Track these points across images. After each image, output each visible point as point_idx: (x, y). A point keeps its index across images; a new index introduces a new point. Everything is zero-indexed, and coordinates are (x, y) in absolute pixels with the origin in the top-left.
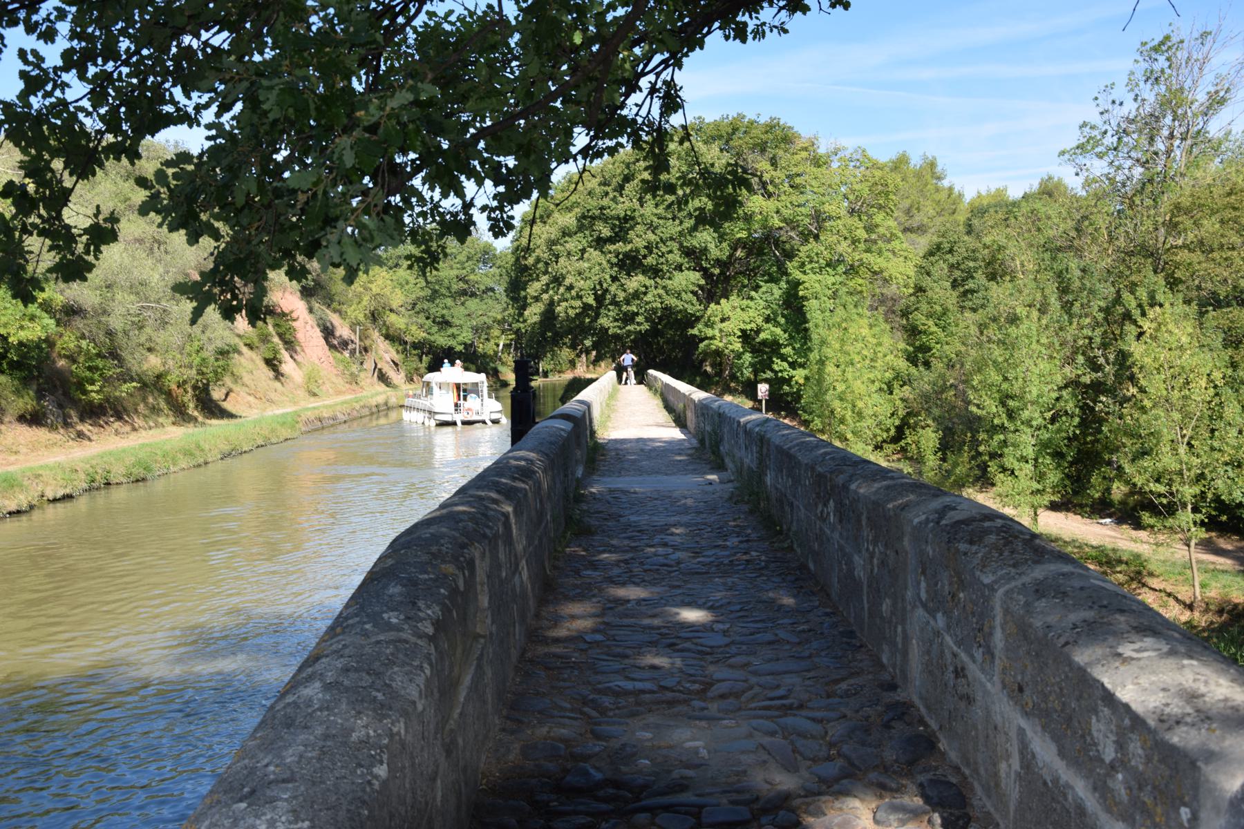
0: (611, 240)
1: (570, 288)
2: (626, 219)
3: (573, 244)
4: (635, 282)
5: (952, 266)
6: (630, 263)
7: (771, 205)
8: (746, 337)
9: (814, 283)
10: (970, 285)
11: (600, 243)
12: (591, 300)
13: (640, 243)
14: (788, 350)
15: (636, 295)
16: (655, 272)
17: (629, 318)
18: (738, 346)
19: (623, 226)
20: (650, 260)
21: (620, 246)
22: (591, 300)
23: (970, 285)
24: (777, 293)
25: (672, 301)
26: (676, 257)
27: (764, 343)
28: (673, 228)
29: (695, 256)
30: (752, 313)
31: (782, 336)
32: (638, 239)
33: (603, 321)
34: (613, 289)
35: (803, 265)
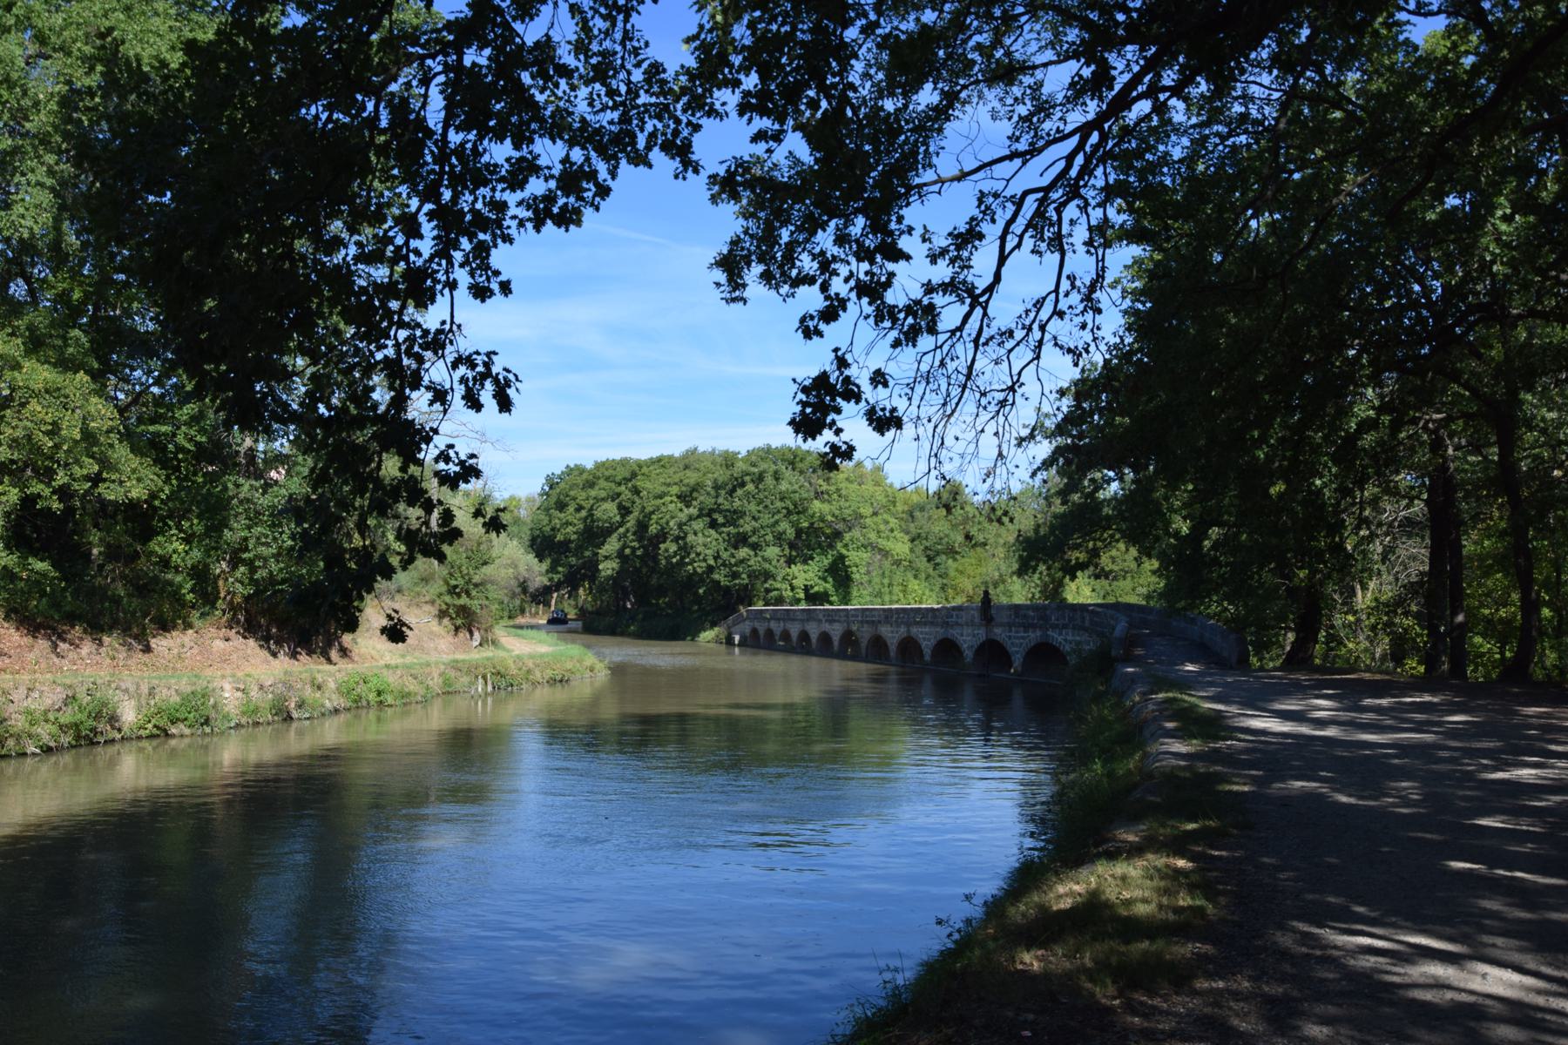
0: (724, 525)
1: (698, 554)
2: (735, 512)
3: (698, 525)
4: (744, 552)
5: (926, 548)
6: (741, 540)
7: (826, 508)
8: (806, 589)
9: (854, 557)
10: (938, 560)
11: (713, 525)
12: (712, 562)
13: (748, 528)
14: (834, 598)
15: (742, 561)
16: (755, 547)
17: (735, 575)
18: (802, 595)
19: (734, 517)
20: (754, 539)
21: (731, 529)
22: (712, 562)
23: (938, 560)
24: (826, 562)
25: (767, 566)
26: (769, 537)
27: (817, 593)
28: (766, 519)
29: (779, 538)
30: (811, 574)
31: (831, 590)
32: (747, 526)
33: (716, 576)
34: (725, 555)
35: (846, 546)
